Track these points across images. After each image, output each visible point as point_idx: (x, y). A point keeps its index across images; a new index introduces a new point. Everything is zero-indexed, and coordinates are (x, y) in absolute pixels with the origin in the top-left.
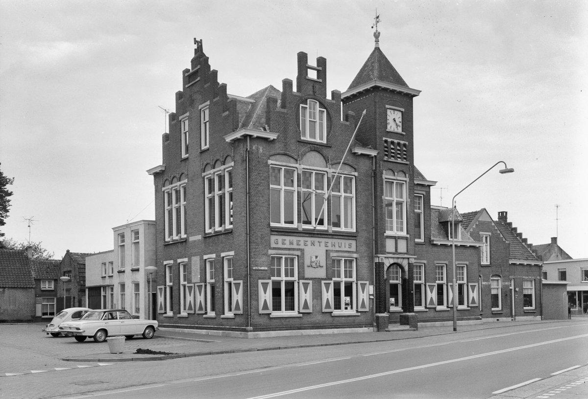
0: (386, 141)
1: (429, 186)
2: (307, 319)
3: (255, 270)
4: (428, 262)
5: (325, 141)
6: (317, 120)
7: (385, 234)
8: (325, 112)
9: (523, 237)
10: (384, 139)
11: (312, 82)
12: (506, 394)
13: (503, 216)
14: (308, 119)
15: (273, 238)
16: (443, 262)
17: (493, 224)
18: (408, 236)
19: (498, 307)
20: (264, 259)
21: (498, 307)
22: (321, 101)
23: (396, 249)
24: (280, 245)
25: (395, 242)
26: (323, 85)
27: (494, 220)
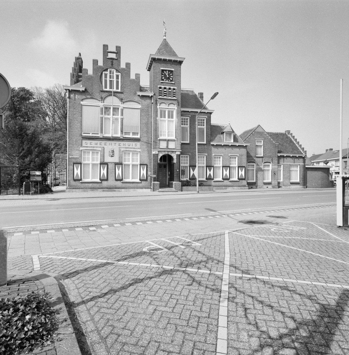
0: (160, 88)
1: (211, 113)
2: (105, 183)
3: (72, 158)
4: (208, 154)
5: (119, 90)
6: (115, 79)
7: (158, 139)
8: (105, 72)
9: (297, 141)
10: (159, 86)
11: (111, 60)
12: (67, 225)
13: (18, 88)
14: (108, 79)
15: (84, 142)
16: (297, 164)
17: (266, 133)
18: (176, 139)
19: (254, 180)
20: (77, 152)
21: (254, 180)
22: (117, 69)
23: (167, 147)
24: (89, 145)
25: (171, 142)
26: (118, 59)
27: (266, 131)
